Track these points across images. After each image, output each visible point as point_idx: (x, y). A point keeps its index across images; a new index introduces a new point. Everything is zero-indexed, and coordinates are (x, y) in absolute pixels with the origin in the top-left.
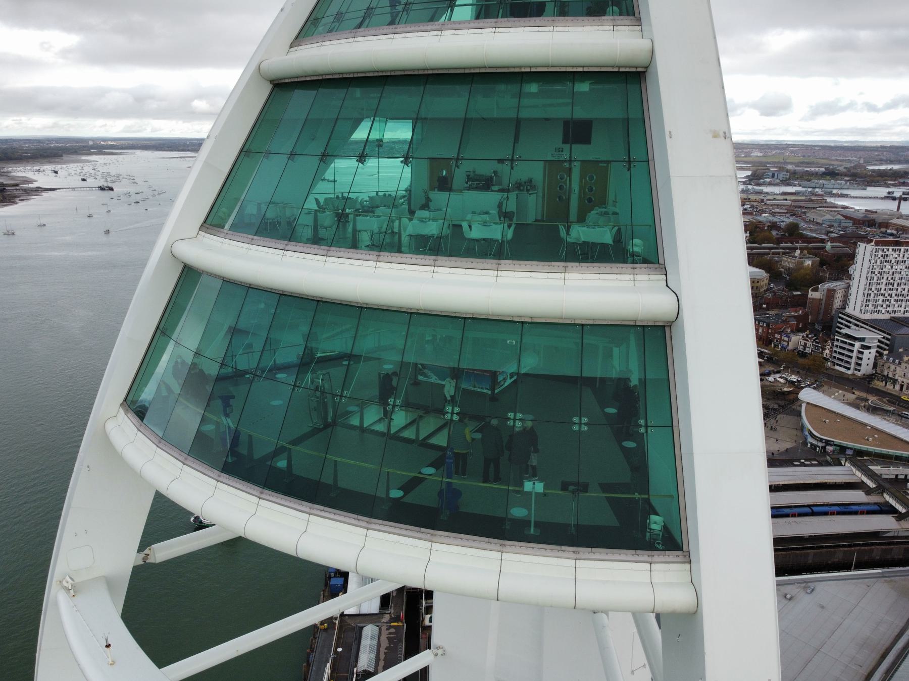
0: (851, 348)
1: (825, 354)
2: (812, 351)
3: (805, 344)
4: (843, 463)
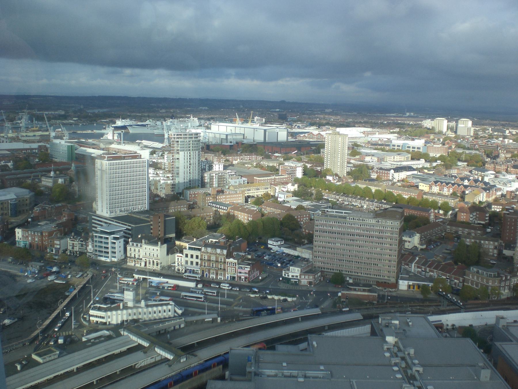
0: (106, 241)
1: (89, 249)
2: (79, 248)
3: (73, 244)
4: (122, 333)
